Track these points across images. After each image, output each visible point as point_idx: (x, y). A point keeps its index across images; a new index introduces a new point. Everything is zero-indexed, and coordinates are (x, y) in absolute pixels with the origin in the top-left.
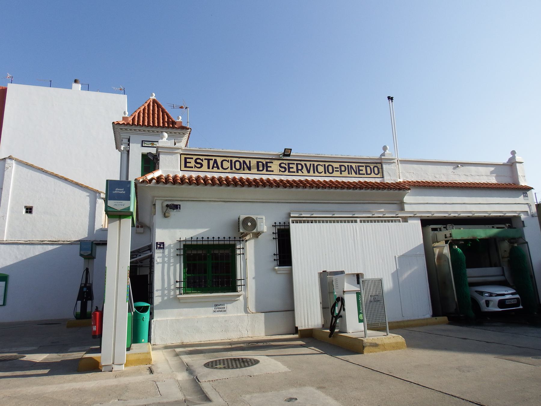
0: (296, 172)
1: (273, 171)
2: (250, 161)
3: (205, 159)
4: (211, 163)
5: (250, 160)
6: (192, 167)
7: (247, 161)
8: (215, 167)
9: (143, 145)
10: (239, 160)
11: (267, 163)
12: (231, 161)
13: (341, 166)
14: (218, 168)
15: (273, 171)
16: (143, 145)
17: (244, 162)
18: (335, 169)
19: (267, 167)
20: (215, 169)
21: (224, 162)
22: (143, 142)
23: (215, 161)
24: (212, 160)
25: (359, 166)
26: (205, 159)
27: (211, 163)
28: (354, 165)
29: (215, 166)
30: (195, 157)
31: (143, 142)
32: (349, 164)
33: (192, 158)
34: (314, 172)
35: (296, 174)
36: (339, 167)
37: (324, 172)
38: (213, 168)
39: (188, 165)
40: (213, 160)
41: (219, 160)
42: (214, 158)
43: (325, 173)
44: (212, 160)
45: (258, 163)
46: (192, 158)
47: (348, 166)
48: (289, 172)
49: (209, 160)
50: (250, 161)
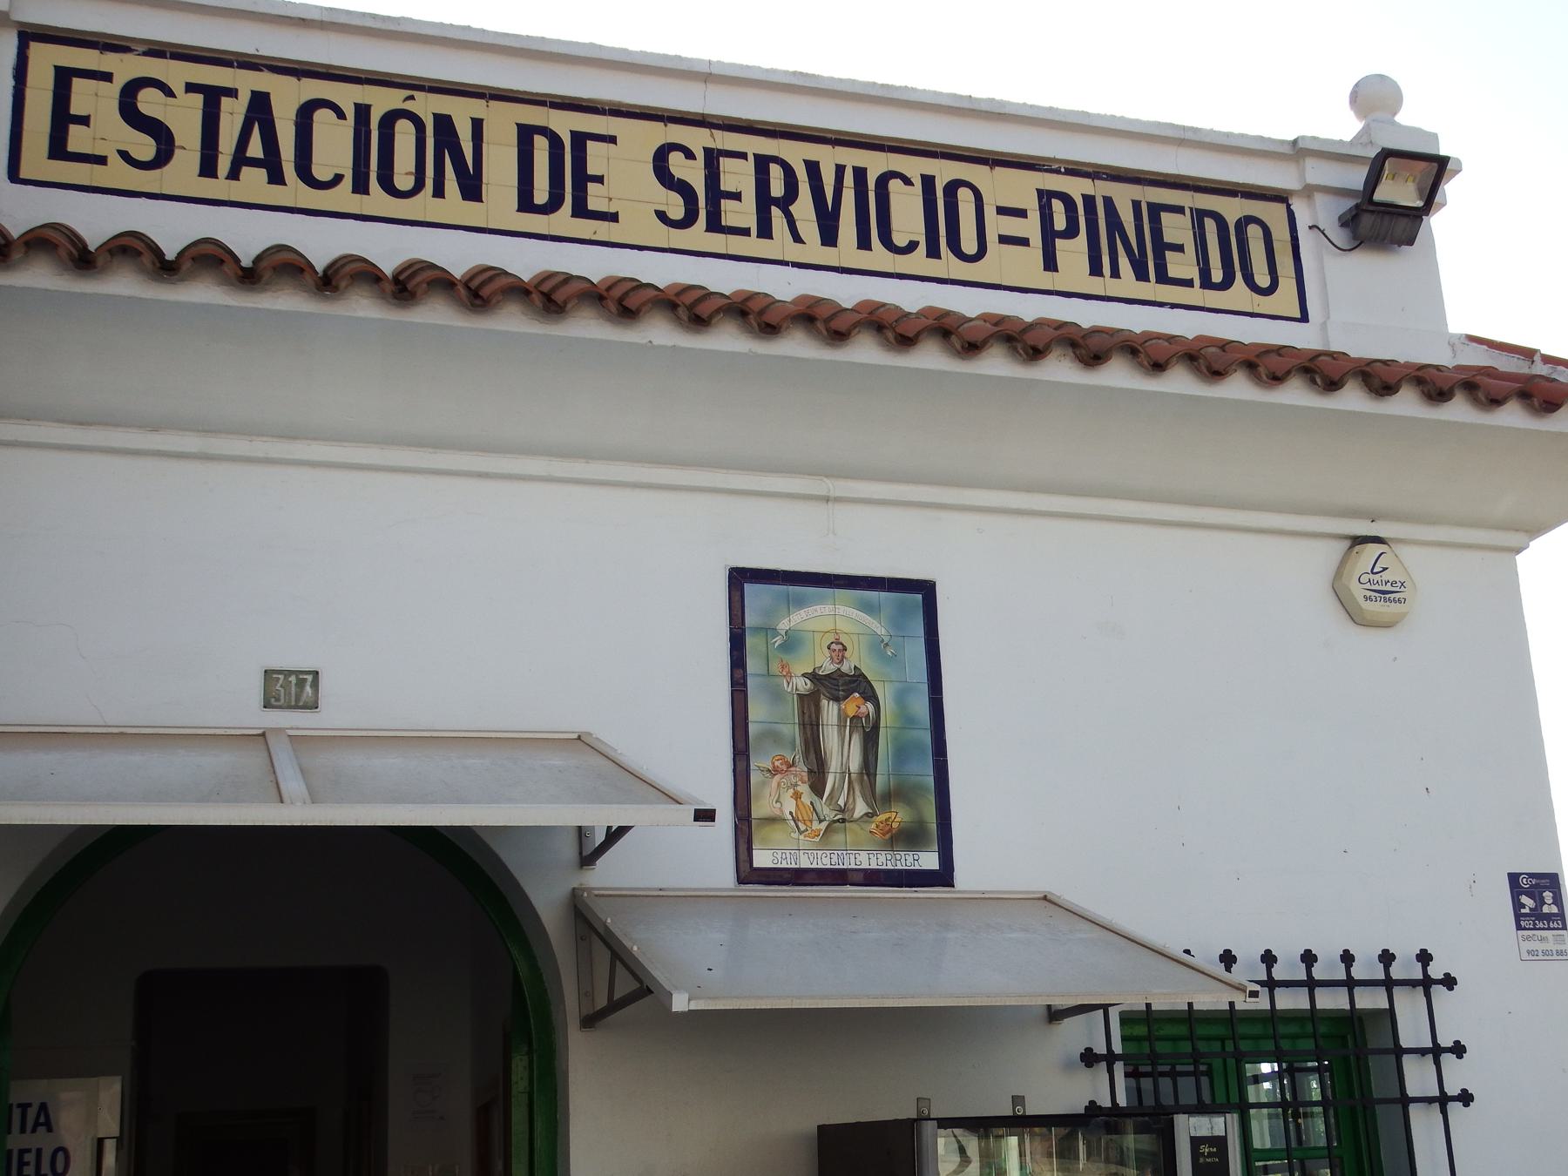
0: (754, 232)
1: (613, 217)
2: (477, 125)
3: (191, 88)
4: (232, 115)
5: (476, 108)
6: (101, 160)
7: (462, 112)
8: (254, 163)
10: (409, 106)
11: (580, 139)
13: (1045, 197)
14: (276, 177)
15: (613, 217)
17: (444, 124)
18: (997, 225)
19: (583, 179)
20: (254, 181)
21: (322, 117)
23: (260, 106)
24: (232, 93)
25: (1156, 210)
26: (191, 88)
27: (232, 115)
28: (1123, 196)
29: (255, 149)
30: (126, 68)
32: (1100, 189)
33: (107, 77)
34: (864, 243)
35: (752, 245)
36: (1032, 204)
37: (922, 248)
38: (234, 175)
39: (78, 139)
40: (244, 98)
41: (287, 97)
42: (246, 82)
43: (934, 252)
44: (232, 93)
45: (526, 134)
46: (107, 77)
47: (1089, 201)
48: (715, 225)
49: (213, 97)
50: (477, 125)
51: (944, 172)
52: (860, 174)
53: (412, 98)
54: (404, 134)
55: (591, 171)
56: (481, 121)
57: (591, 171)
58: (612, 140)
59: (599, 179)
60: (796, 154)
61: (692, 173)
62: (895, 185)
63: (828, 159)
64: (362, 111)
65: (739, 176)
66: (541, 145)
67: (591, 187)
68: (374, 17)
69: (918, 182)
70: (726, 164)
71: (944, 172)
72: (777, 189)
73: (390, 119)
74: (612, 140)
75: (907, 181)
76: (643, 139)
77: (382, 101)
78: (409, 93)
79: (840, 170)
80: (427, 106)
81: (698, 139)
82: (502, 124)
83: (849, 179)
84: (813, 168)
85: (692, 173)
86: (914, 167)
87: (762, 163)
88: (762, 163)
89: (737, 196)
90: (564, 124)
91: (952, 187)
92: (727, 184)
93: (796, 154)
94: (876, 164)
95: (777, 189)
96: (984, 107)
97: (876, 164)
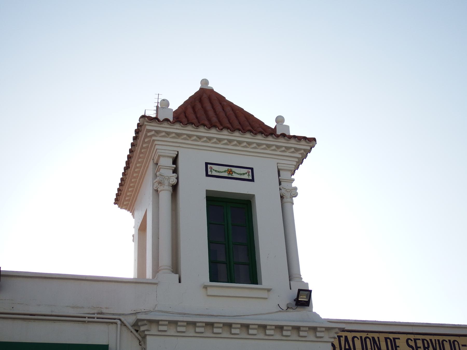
2: (378, 338)
4: (343, 340)
7: (376, 336)
9: (209, 173)
10: (368, 336)
11: (394, 339)
12: (361, 337)
16: (209, 173)
17: (373, 338)
21: (356, 339)
22: (209, 166)
27: (343, 340)
31: (209, 166)
41: (350, 336)
44: (342, 336)
45: (386, 339)
50: (378, 338)
51: (452, 339)
52: (439, 340)
53: (368, 334)
54: (368, 340)
55: (397, 345)
56: (379, 337)
57: (397, 345)
58: (399, 339)
59: (398, 347)
60: (428, 338)
61: (412, 343)
62: (445, 342)
63: (433, 338)
64: (361, 337)
65: (420, 344)
66: (388, 340)
67: (398, 348)
68: (362, 321)
69: (448, 341)
70: (418, 341)
71: (452, 339)
72: (426, 346)
73: (366, 338)
74: (399, 339)
75: (446, 342)
76: (405, 337)
77: (364, 335)
78: (367, 333)
79: (435, 340)
80: (370, 335)
81: (412, 337)
82: (382, 337)
83: (437, 342)
84: (431, 340)
85: (412, 343)
86: (447, 338)
87: (423, 340)
88: (423, 340)
89: (420, 348)
90: (391, 336)
91: (454, 341)
92: (418, 345)
93: (428, 338)
94: (441, 338)
95: (426, 346)
96: (458, 326)
97: (441, 338)
